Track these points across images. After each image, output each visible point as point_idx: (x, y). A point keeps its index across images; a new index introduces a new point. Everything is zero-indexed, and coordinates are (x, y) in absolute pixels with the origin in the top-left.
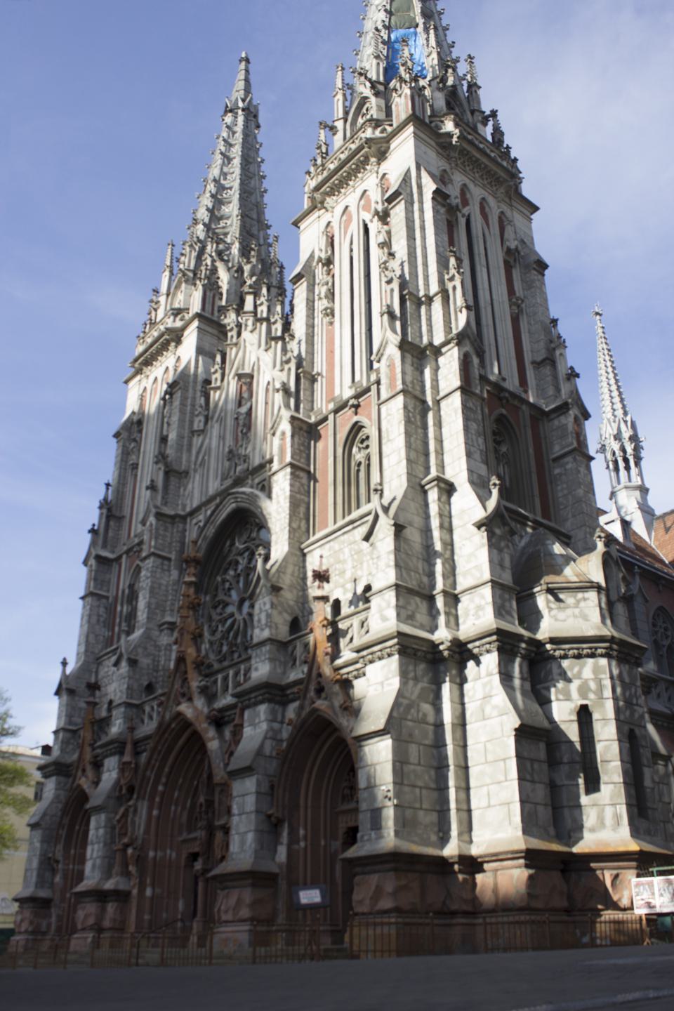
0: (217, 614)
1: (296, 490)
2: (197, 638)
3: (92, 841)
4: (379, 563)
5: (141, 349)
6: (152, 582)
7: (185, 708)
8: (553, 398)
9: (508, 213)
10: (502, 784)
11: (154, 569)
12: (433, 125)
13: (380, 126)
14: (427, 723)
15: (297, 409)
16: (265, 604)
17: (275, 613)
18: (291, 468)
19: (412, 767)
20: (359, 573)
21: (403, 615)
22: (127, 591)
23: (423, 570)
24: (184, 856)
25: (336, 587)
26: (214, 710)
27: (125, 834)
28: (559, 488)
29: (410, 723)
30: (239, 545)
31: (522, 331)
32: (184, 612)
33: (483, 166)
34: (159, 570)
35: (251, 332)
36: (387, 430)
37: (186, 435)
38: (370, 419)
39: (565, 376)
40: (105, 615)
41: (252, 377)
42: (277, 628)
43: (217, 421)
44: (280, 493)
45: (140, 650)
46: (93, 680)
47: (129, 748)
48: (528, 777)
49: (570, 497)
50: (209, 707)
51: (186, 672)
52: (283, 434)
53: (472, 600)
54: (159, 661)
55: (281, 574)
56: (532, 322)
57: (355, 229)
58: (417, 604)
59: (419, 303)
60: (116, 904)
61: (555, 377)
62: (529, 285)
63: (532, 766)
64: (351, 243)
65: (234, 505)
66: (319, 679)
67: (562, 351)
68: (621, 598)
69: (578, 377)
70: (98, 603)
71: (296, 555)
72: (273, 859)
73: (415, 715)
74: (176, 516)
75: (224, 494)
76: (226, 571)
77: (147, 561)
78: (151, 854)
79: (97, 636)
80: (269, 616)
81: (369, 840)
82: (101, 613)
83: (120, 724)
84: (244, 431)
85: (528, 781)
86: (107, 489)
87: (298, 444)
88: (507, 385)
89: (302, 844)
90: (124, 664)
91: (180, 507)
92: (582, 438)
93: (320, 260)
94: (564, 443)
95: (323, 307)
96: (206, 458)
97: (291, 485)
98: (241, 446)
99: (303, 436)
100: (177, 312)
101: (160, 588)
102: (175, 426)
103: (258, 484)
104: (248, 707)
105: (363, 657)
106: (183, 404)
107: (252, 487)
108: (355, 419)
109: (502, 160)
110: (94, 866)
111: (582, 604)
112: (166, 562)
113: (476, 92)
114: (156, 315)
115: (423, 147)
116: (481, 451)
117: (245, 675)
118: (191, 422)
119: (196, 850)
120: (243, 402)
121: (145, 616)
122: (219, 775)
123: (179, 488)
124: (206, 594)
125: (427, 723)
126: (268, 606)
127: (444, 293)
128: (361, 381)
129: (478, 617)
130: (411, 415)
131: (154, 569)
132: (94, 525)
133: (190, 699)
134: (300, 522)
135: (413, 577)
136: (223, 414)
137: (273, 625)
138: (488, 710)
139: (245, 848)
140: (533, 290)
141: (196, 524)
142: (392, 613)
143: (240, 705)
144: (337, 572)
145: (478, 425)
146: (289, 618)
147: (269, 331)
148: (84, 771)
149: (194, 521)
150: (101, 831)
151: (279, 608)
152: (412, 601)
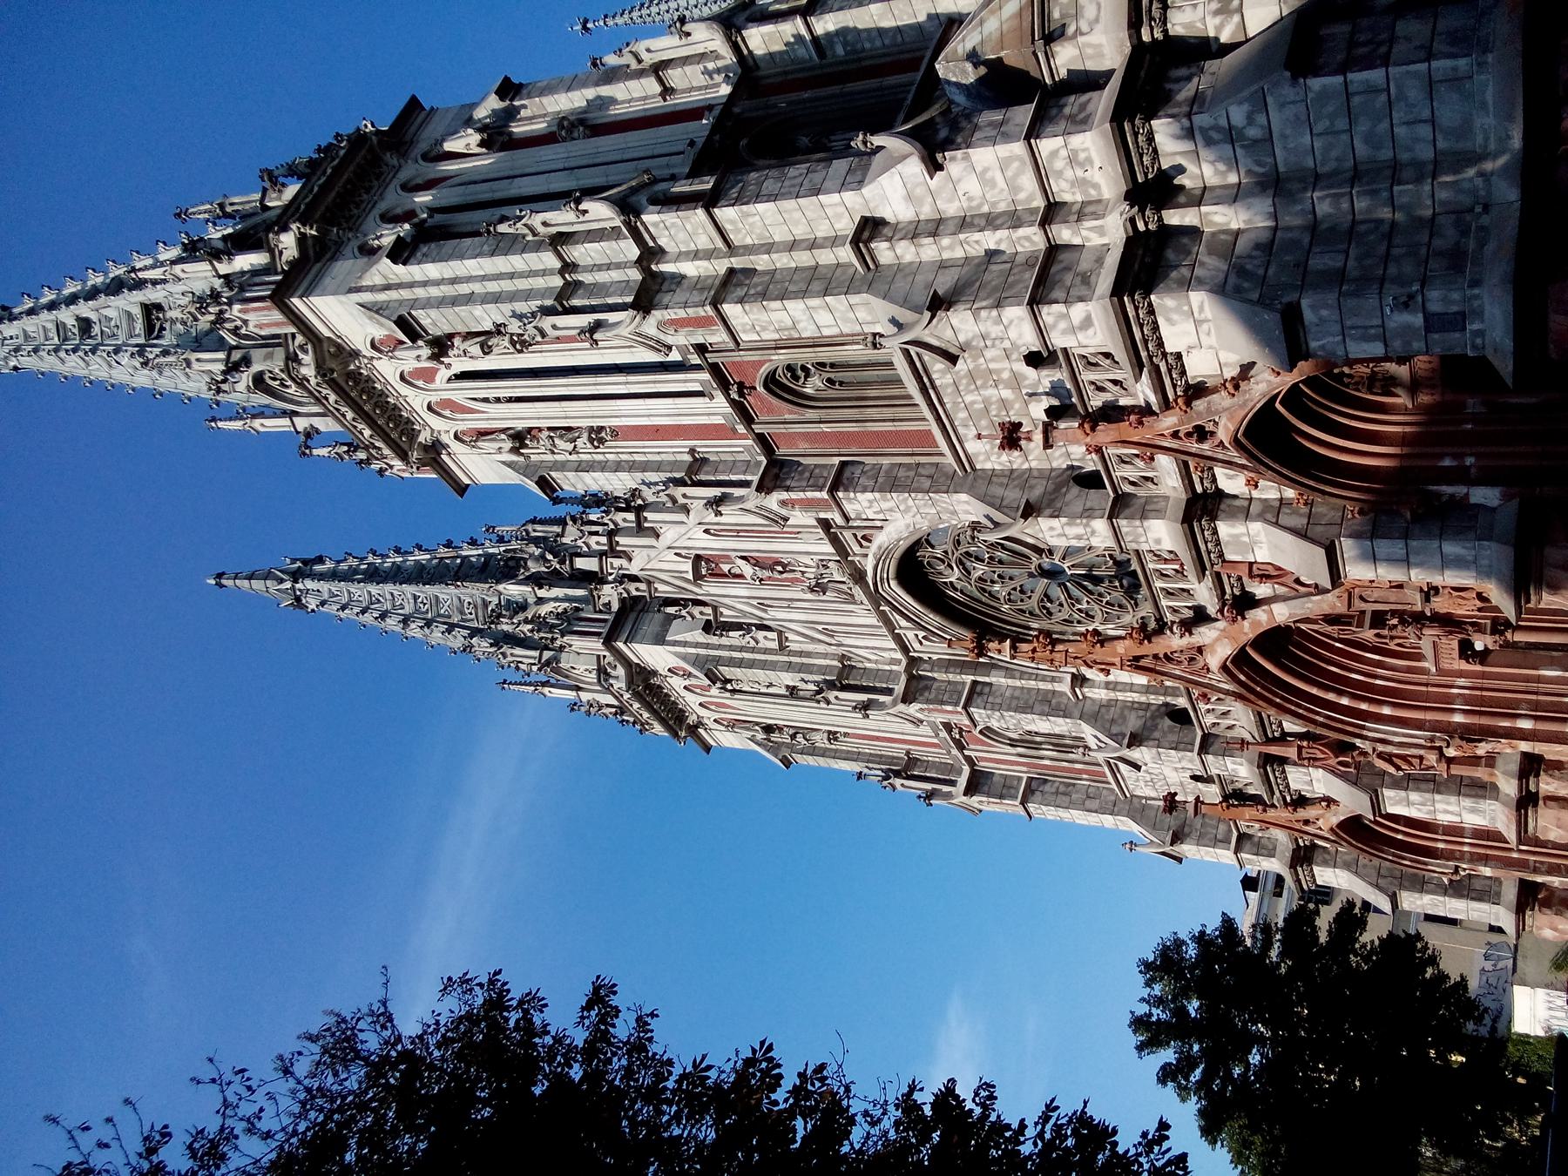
2: (1101, 639)
3: (1429, 812)
4: (993, 336)
5: (658, 728)
6: (1009, 710)
7: (1214, 660)
10: (1393, 97)
11: (989, 706)
13: (296, 355)
14: (1273, 241)
15: (745, 484)
16: (1052, 529)
18: (837, 490)
19: (1351, 263)
20: (1006, 375)
21: (1084, 291)
22: (1020, 750)
24: (1464, 666)
25: (1028, 414)
26: (1221, 611)
27: (1421, 758)
29: (1271, 272)
30: (954, 576)
32: (1059, 657)
35: (630, 560)
36: (777, 331)
37: (786, 659)
38: (762, 363)
41: (698, 558)
43: (765, 611)
44: (876, 508)
45: (1115, 730)
46: (1161, 803)
47: (1274, 750)
48: (1383, 49)
50: (1217, 620)
51: (1156, 657)
52: (783, 503)
53: (1060, 174)
54: (1133, 702)
55: (1004, 503)
59: (571, 288)
60: (1543, 777)
63: (1364, 44)
64: (486, 400)
66: (1181, 435)
70: (1038, 793)
72: (1494, 510)
73: (1256, 262)
74: (908, 669)
75: (876, 598)
77: (976, 717)
78: (1458, 718)
79: (1088, 797)
81: (1480, 333)
82: (1054, 790)
83: (1234, 763)
84: (780, 568)
85: (1391, 48)
89: (1469, 461)
91: (895, 668)
93: (515, 450)
95: (589, 445)
96: (820, 627)
97: (864, 491)
98: (803, 573)
99: (787, 473)
100: (603, 673)
101: (1018, 698)
102: (771, 676)
103: (861, 546)
104: (1221, 555)
105: (1150, 357)
106: (740, 663)
108: (760, 389)
110: (1473, 811)
112: (979, 688)
114: (608, 706)
117: (1166, 561)
118: (766, 651)
119: (1455, 644)
120: (737, 571)
121: (1060, 720)
122: (1332, 603)
125: (1273, 241)
126: (1055, 523)
127: (559, 240)
128: (702, 382)
129: (1089, 160)
133: (1200, 650)
135: (1017, 277)
136: (755, 602)
138: (1253, 132)
139: (1470, 558)
141: (921, 643)
142: (1078, 311)
143: (1216, 568)
146: (1075, 490)
147: (628, 532)
148: (1307, 822)
149: (917, 646)
150: (1414, 796)
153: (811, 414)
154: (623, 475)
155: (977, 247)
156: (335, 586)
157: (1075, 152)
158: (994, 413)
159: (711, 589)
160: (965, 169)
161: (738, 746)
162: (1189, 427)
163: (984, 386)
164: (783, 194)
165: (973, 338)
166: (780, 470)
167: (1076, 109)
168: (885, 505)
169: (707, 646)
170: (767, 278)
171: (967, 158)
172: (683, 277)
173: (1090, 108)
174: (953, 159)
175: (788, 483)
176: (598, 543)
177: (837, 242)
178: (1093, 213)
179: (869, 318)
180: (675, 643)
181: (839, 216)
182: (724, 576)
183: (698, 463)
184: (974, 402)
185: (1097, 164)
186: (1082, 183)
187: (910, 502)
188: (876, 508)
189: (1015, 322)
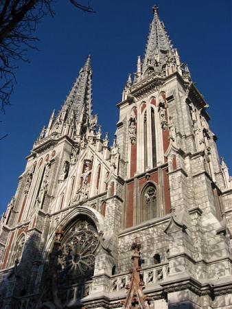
16: (102, 257)
20: (152, 248)
30: (77, 230)
52: (113, 183)
57: (148, 109)
64: (145, 115)
74: (48, 214)
76: (69, 241)
90: (14, 277)
100: (56, 134)
106: (55, 169)
118: (58, 177)
126: (104, 259)
129: (221, 275)
153: (139, 194)
154: (122, 144)
156: (85, 80)
157: (224, 271)
159: (80, 164)
161: (27, 166)
162: (138, 299)
163: (148, 242)
168: (110, 211)
169: (61, 161)
183: (124, 162)
185: (220, 277)
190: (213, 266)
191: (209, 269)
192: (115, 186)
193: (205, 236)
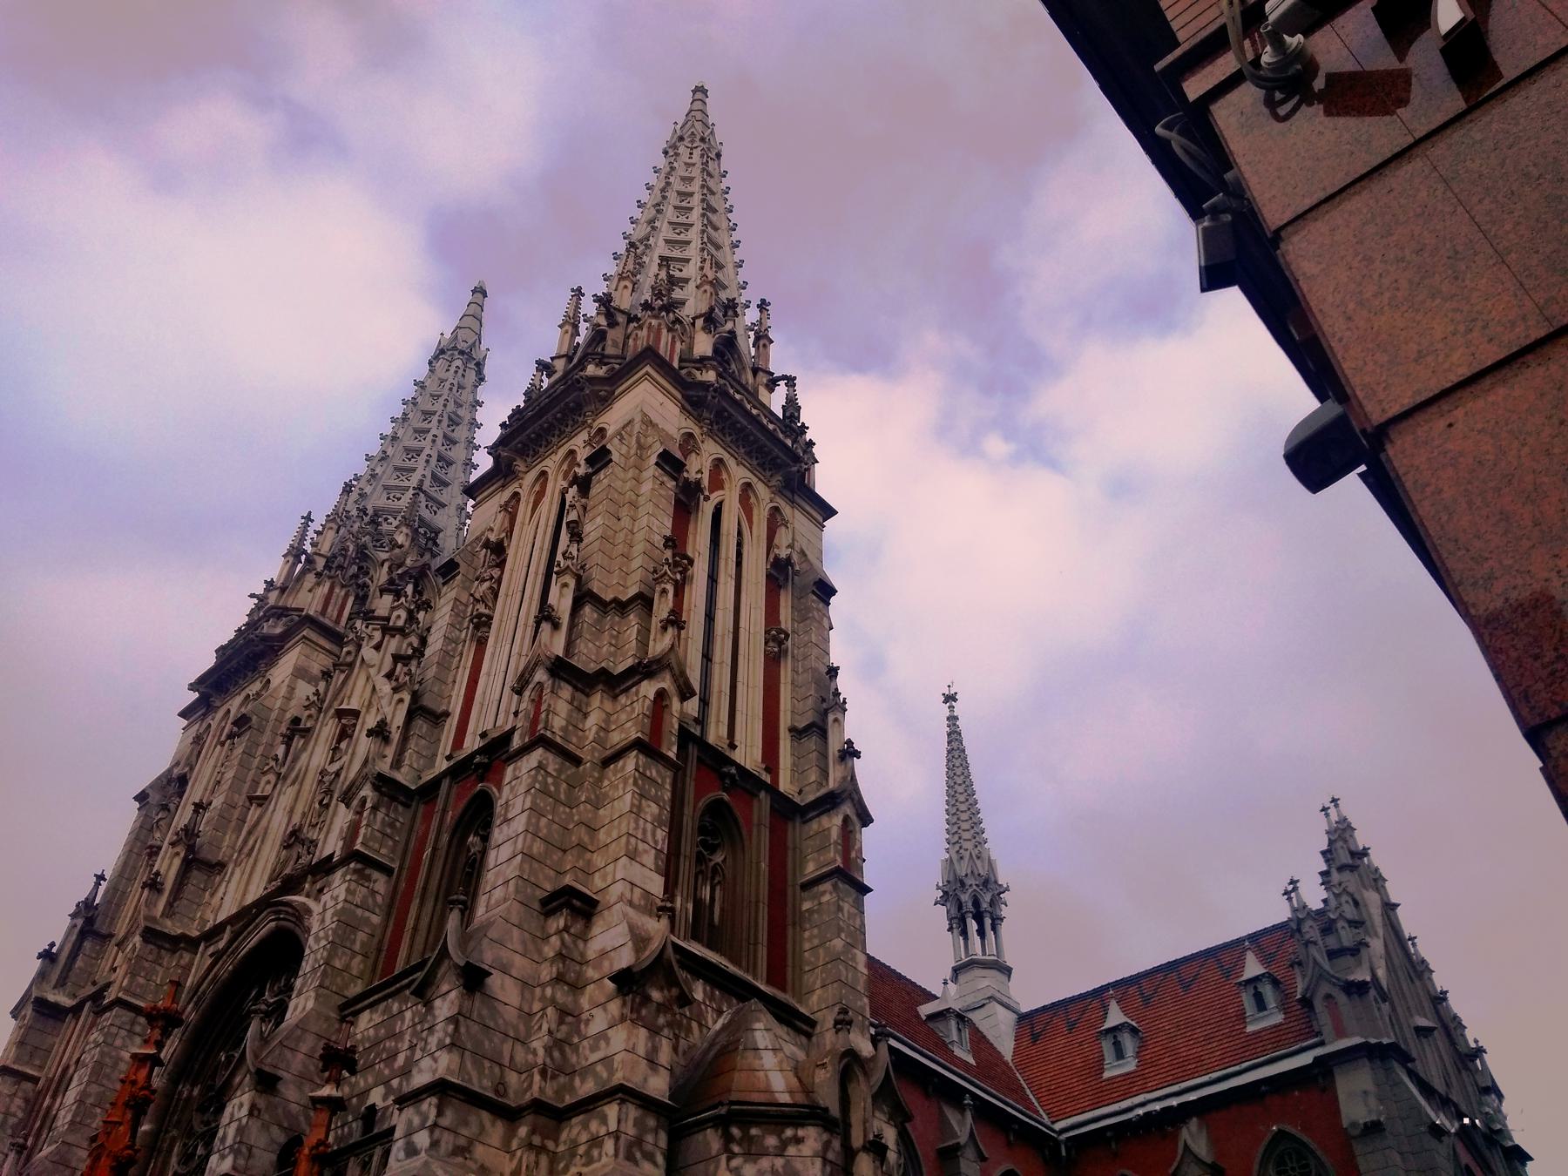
0: (202, 1122)
1: (358, 900)
4: (430, 1040)
6: (102, 1054)
8: (814, 785)
9: (787, 510)
12: (683, 372)
15: (397, 764)
16: (241, 1105)
17: (255, 1125)
23: (512, 1058)
28: (807, 934)
31: (782, 680)
33: (752, 438)
34: (123, 1033)
39: (837, 754)
40: (20, 1114)
42: (250, 1155)
49: (821, 951)
52: (364, 801)
53: (586, 1126)
56: (800, 670)
58: (482, 1128)
61: (824, 755)
62: (802, 615)
65: (273, 924)
67: (839, 716)
68: (871, 1142)
69: (859, 757)
71: (327, 1019)
74: (184, 938)
75: (263, 904)
77: (108, 1014)
80: (241, 1130)
82: (13, 1109)
86: (98, 884)
87: (383, 820)
88: (738, 756)
92: (853, 855)
94: (822, 858)
97: (348, 890)
99: (396, 809)
101: (116, 1064)
107: (308, 896)
109: (787, 436)
111: (791, 1150)
113: (764, 346)
115: (661, 397)
116: (659, 851)
118: (256, 783)
123: (204, 890)
124: (193, 1085)
126: (245, 1111)
129: (590, 1161)
130: (550, 780)
131: (114, 1030)
132: (52, 945)
134: (352, 959)
135: (487, 1071)
137: (244, 1150)
140: (808, 622)
144: (384, 1056)
145: (661, 808)
146: (281, 1138)
151: (266, 1117)
152: (473, 1119)
153: (445, 838)
155: (536, 1027)
158: (388, 1044)
160: (613, 1017)
163: (415, 1034)
164: (636, 822)
165: (434, 1017)
166: (402, 804)
167: (649, 1148)
168: (329, 914)
170: (562, 797)
171: (623, 1019)
172: (586, 715)
173: (647, 1166)
174: (624, 1004)
175: (383, 810)
176: (399, 617)
177: (580, 874)
178: (537, 1163)
179: (493, 901)
180: (292, 689)
181: (604, 878)
182: (339, 741)
184: (403, 1022)
185: (584, 1170)
186: (572, 1152)
187: (323, 943)
188: (331, 903)
189: (434, 1066)
190: (575, 1131)
191: (564, 1136)
192: (366, 814)
193: (584, 1002)
